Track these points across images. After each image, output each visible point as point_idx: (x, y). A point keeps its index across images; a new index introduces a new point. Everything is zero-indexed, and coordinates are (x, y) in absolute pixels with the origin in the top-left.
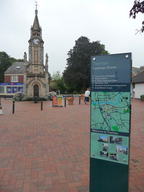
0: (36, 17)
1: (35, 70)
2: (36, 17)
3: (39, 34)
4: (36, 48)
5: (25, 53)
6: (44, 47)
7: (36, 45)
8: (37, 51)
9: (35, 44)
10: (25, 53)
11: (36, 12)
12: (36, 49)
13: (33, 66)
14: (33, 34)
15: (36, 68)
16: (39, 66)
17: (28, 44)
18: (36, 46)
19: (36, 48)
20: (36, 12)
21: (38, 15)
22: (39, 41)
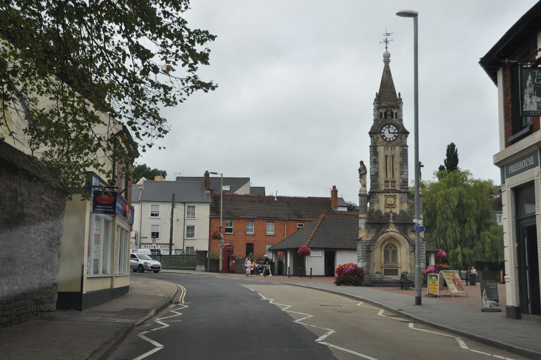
0: (387, 73)
1: (388, 206)
2: (387, 73)
3: (396, 114)
4: (389, 148)
5: (362, 163)
6: (408, 145)
7: (390, 141)
8: (393, 157)
9: (385, 140)
10: (362, 163)
11: (387, 59)
12: (389, 152)
13: (383, 195)
14: (381, 114)
15: (390, 200)
16: (398, 194)
17: (368, 141)
18: (388, 143)
19: (389, 148)
20: (387, 59)
21: (391, 65)
22: (396, 131)
